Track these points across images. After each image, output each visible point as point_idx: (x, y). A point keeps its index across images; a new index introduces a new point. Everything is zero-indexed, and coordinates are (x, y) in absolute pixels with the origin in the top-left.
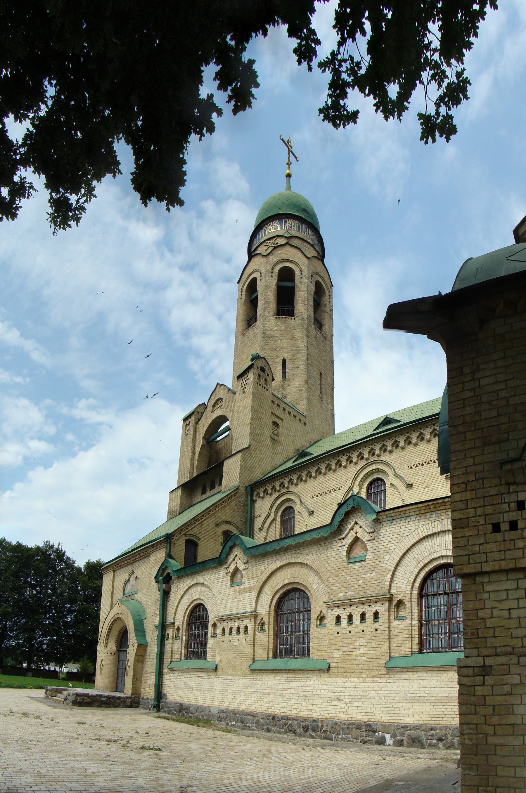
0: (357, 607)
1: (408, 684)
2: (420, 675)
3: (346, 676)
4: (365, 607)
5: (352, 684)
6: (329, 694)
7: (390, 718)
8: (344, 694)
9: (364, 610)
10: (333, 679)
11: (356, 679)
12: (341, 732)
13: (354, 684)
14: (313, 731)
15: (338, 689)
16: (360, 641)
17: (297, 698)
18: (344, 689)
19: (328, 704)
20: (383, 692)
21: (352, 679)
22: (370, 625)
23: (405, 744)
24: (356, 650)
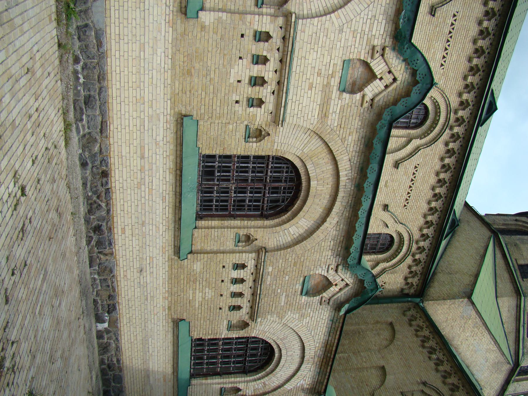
0: (251, 288)
1: (161, 338)
2: (170, 348)
3: (170, 278)
4: (249, 297)
5: (161, 285)
6: (148, 258)
7: (125, 323)
8: (148, 276)
9: (246, 295)
10: (167, 263)
11: (167, 289)
12: (102, 278)
13: (161, 288)
14: (97, 242)
15: (155, 269)
16: (210, 293)
17: (140, 211)
18: (155, 276)
19: (135, 257)
20: (153, 317)
21: (167, 285)
22: (228, 301)
23: (101, 341)
24: (201, 289)
